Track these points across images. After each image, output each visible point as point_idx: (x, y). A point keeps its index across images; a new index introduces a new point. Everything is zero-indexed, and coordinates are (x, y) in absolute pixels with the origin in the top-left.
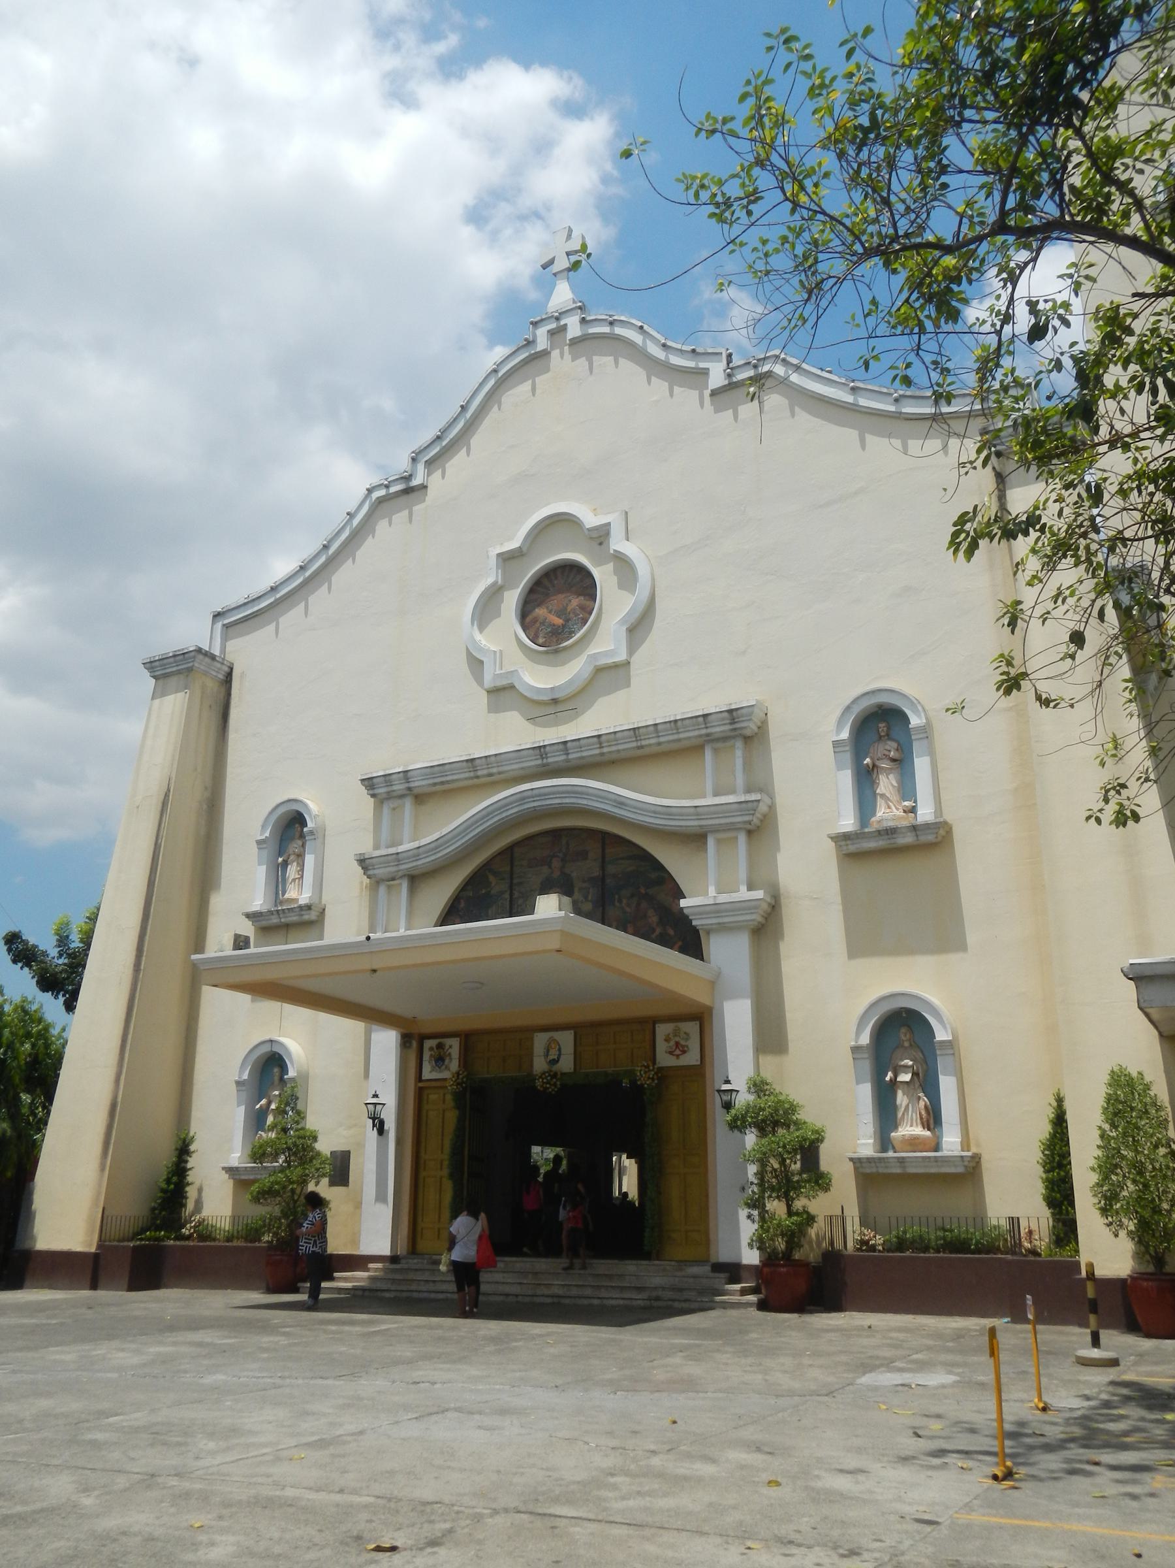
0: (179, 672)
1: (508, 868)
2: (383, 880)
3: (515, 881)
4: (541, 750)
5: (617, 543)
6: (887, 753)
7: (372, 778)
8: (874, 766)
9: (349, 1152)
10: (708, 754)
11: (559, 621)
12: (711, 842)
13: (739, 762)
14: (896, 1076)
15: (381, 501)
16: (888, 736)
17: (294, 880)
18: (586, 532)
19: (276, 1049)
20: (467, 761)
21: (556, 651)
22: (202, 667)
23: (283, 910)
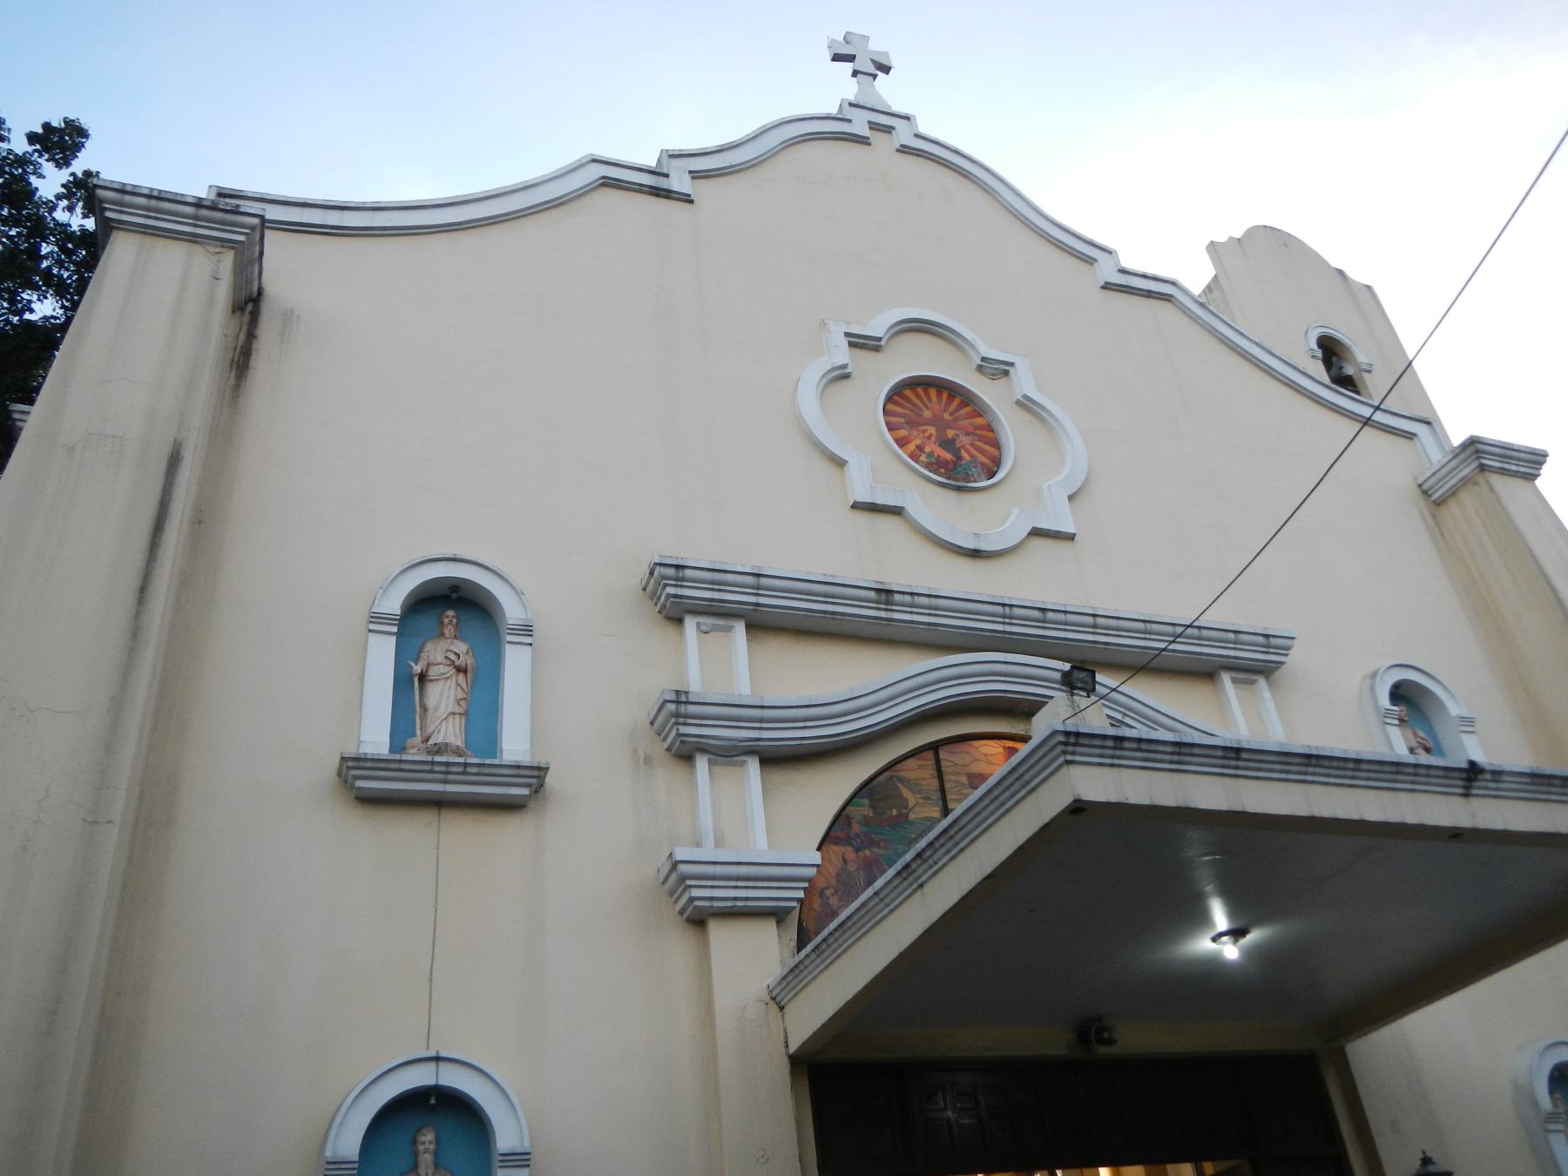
0: (194, 239)
1: (935, 782)
7: (683, 567)
11: (948, 456)
13: (1271, 706)
15: (608, 183)
17: (453, 713)
18: (979, 362)
19: (452, 1078)
20: (878, 591)
21: (958, 489)
23: (466, 765)
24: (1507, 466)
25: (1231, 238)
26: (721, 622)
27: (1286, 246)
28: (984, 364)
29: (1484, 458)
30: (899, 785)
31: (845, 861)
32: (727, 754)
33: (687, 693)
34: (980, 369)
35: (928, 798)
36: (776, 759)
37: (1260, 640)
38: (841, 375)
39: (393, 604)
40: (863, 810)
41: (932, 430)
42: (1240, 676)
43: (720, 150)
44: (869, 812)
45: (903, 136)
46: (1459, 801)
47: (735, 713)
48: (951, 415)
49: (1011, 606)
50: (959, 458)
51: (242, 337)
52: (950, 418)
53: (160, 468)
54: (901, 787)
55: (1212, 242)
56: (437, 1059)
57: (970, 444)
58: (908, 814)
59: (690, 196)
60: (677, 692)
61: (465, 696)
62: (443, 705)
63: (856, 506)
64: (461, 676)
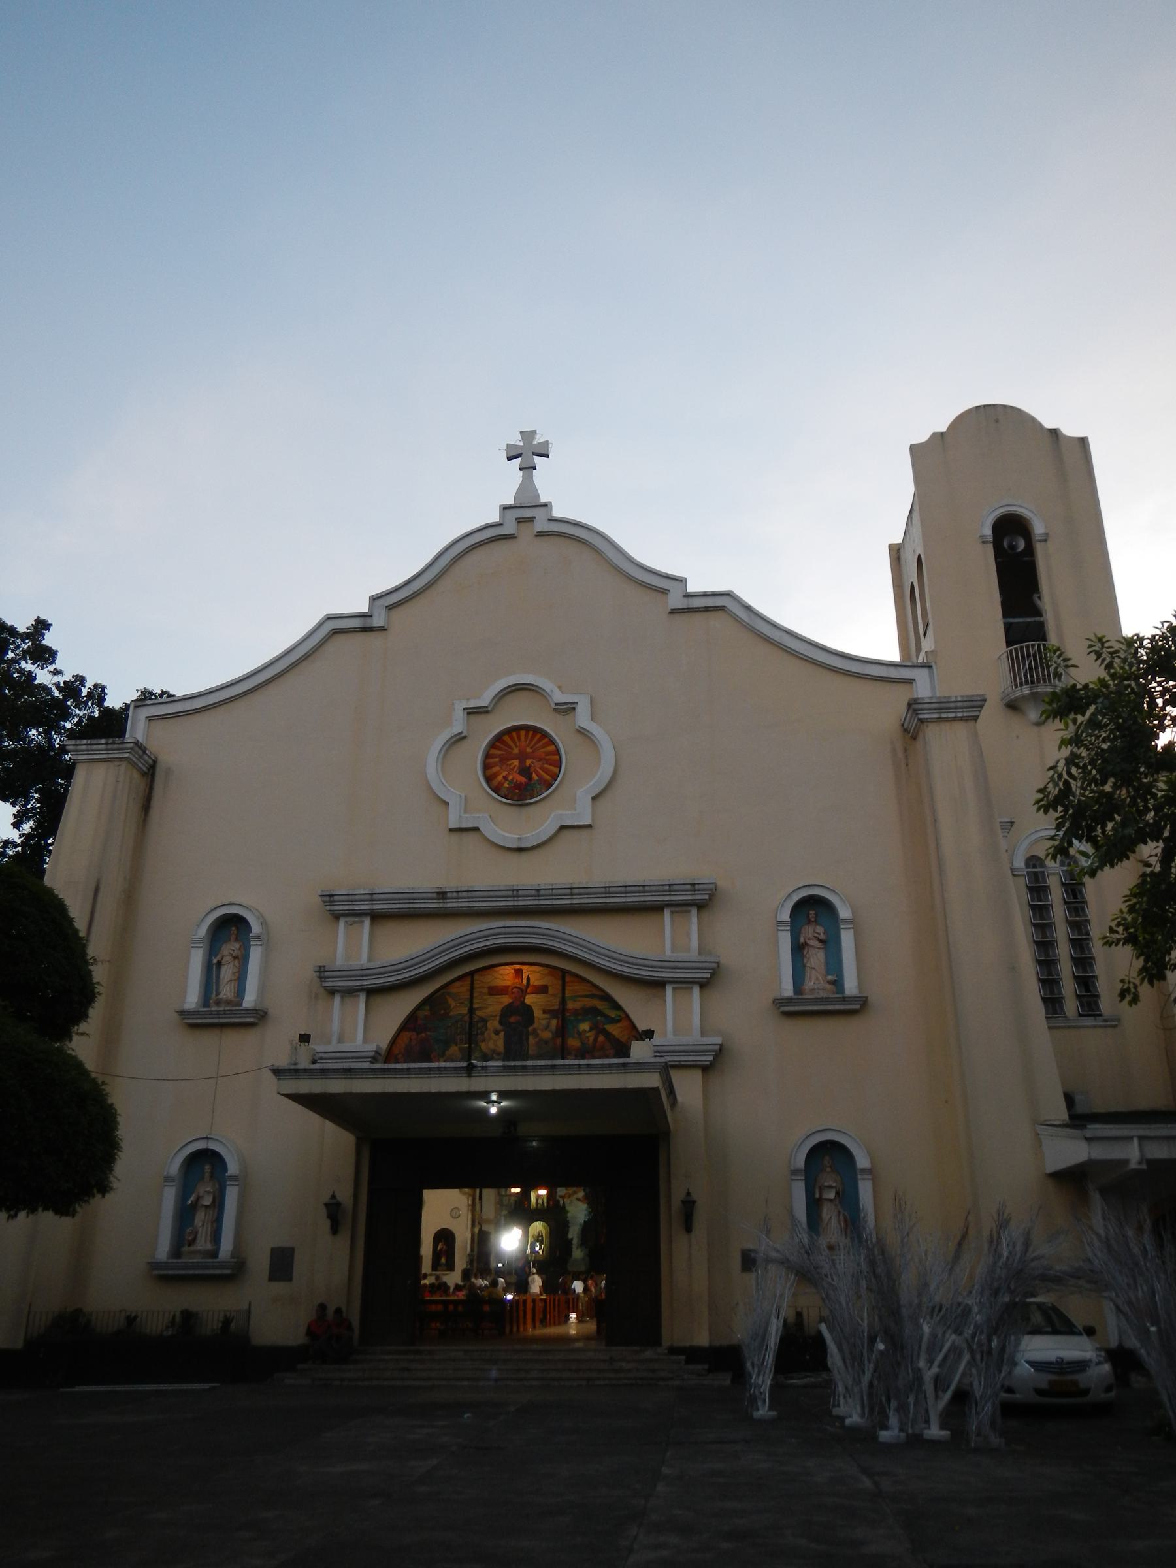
1: (467, 995)
2: (338, 991)
3: (475, 1006)
4: (515, 893)
5: (582, 718)
6: (817, 935)
7: (333, 896)
8: (805, 942)
9: (292, 1250)
10: (667, 913)
11: (522, 779)
12: (669, 990)
13: (694, 928)
14: (821, 1194)
15: (336, 632)
17: (231, 981)
18: (553, 706)
19: (213, 1146)
20: (438, 893)
22: (134, 759)
23: (225, 1011)
24: (944, 715)
25: (934, 434)
26: (357, 919)
27: (997, 421)
28: (557, 707)
29: (921, 714)
30: (447, 997)
31: (411, 1039)
32: (349, 993)
33: (324, 966)
34: (555, 710)
35: (462, 1003)
36: (372, 992)
37: (688, 887)
38: (460, 738)
39: (203, 932)
40: (426, 1011)
41: (516, 763)
42: (673, 909)
43: (408, 582)
44: (428, 1013)
45: (541, 525)
46: (468, 1079)
47: (349, 973)
48: (531, 748)
49: (517, 890)
50: (530, 779)
51: (147, 790)
52: (531, 751)
53: (91, 894)
54: (447, 997)
55: (911, 446)
56: (207, 1138)
57: (540, 768)
58: (449, 1012)
59: (383, 627)
60: (320, 967)
61: (237, 970)
62: (226, 977)
63: (451, 830)
64: (236, 961)
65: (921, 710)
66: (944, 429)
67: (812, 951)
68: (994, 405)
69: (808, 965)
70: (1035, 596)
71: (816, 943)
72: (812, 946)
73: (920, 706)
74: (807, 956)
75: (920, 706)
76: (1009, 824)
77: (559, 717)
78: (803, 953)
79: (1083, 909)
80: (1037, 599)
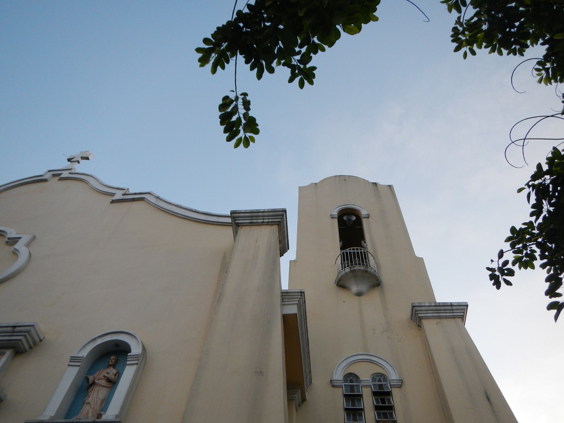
6: (106, 375)
16: (114, 366)
18: (6, 240)
25: (312, 184)
27: (345, 180)
37: (10, 329)
65: (238, 217)
66: (317, 182)
67: (96, 388)
68: (344, 176)
69: (87, 402)
70: (362, 242)
71: (103, 382)
72: (98, 385)
73: (237, 215)
74: (90, 394)
75: (237, 215)
76: (300, 294)
77: (8, 247)
78: (88, 390)
79: (391, 415)
80: (364, 243)
